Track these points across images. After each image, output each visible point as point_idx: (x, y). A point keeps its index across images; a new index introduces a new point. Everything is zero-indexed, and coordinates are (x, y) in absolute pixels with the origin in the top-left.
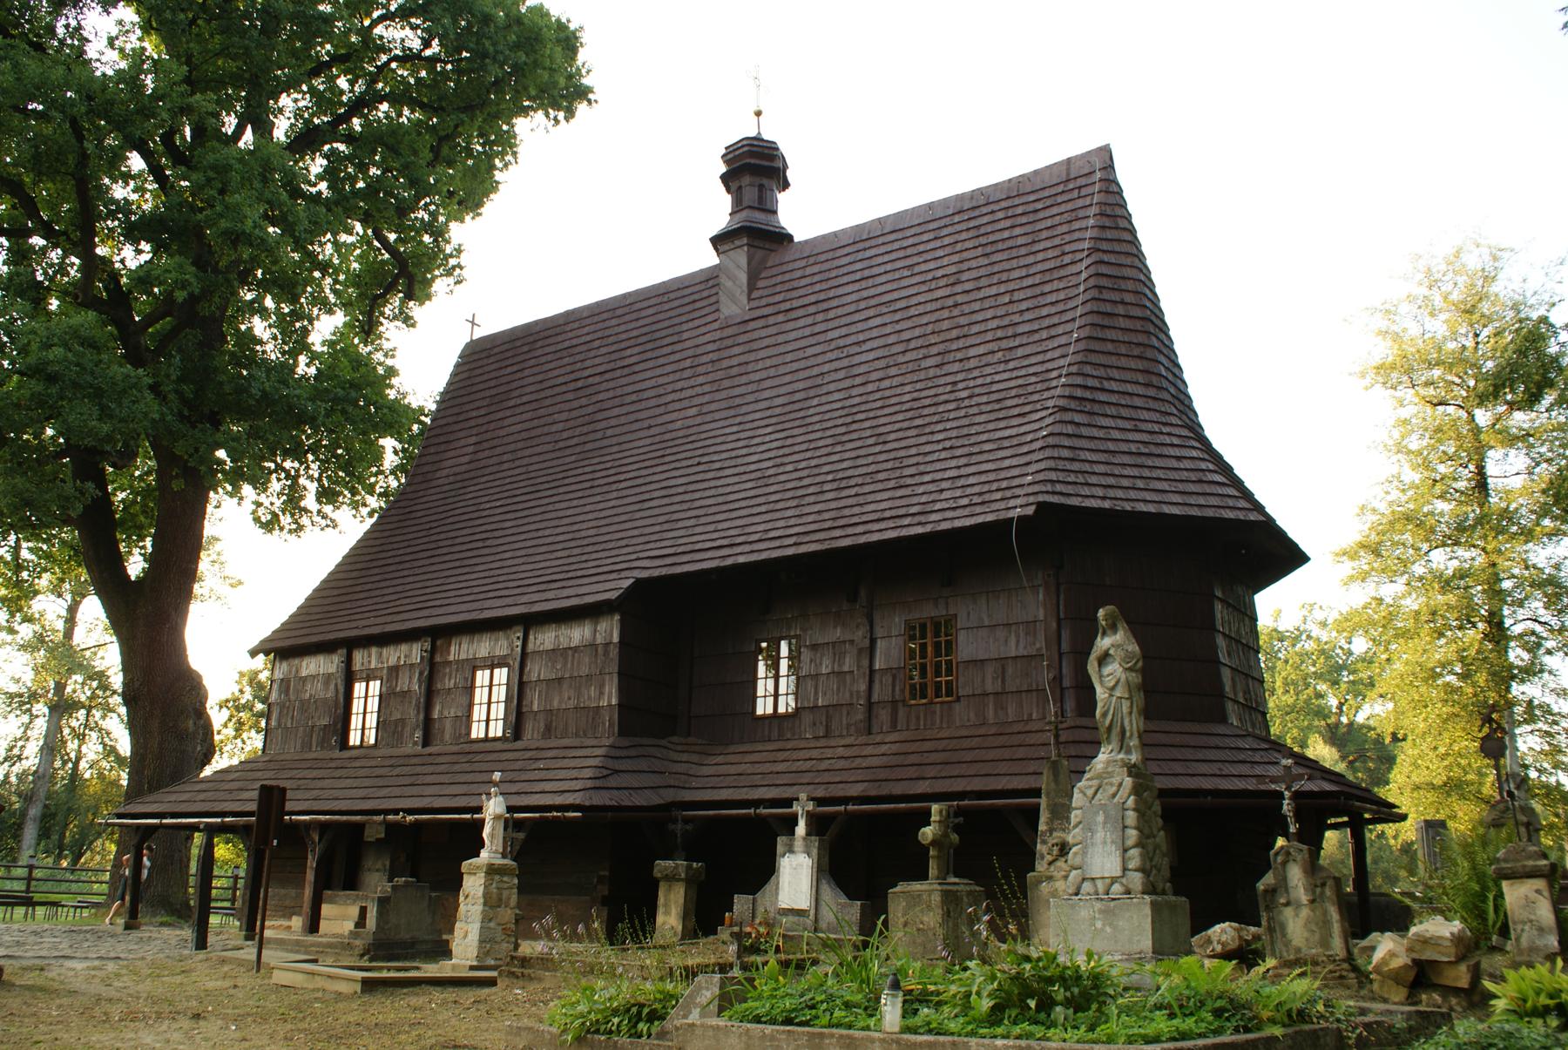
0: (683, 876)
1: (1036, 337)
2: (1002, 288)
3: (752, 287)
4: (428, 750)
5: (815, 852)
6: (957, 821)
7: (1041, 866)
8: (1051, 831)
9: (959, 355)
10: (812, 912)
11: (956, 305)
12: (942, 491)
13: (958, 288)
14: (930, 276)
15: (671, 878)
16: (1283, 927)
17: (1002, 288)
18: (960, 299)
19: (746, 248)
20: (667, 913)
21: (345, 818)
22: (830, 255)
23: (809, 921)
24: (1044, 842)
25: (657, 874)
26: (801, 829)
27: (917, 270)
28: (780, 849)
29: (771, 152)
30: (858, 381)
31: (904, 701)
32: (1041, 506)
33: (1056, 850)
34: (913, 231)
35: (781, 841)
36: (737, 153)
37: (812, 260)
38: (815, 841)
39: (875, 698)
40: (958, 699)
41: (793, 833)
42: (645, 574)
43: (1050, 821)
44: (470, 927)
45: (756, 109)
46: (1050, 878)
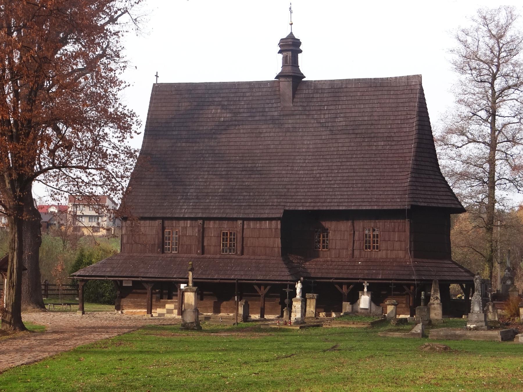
0: (316, 298)
3: (294, 97)
5: (370, 295)
7: (431, 301)
8: (434, 294)
11: (372, 124)
12: (380, 195)
16: (488, 316)
18: (374, 122)
19: (291, 82)
20: (310, 307)
23: (369, 311)
26: (365, 290)
28: (360, 294)
32: (412, 206)
33: (435, 299)
39: (355, 248)
40: (380, 251)
42: (287, 208)
43: (434, 292)
44: (297, 314)
45: (290, 23)
46: (434, 304)
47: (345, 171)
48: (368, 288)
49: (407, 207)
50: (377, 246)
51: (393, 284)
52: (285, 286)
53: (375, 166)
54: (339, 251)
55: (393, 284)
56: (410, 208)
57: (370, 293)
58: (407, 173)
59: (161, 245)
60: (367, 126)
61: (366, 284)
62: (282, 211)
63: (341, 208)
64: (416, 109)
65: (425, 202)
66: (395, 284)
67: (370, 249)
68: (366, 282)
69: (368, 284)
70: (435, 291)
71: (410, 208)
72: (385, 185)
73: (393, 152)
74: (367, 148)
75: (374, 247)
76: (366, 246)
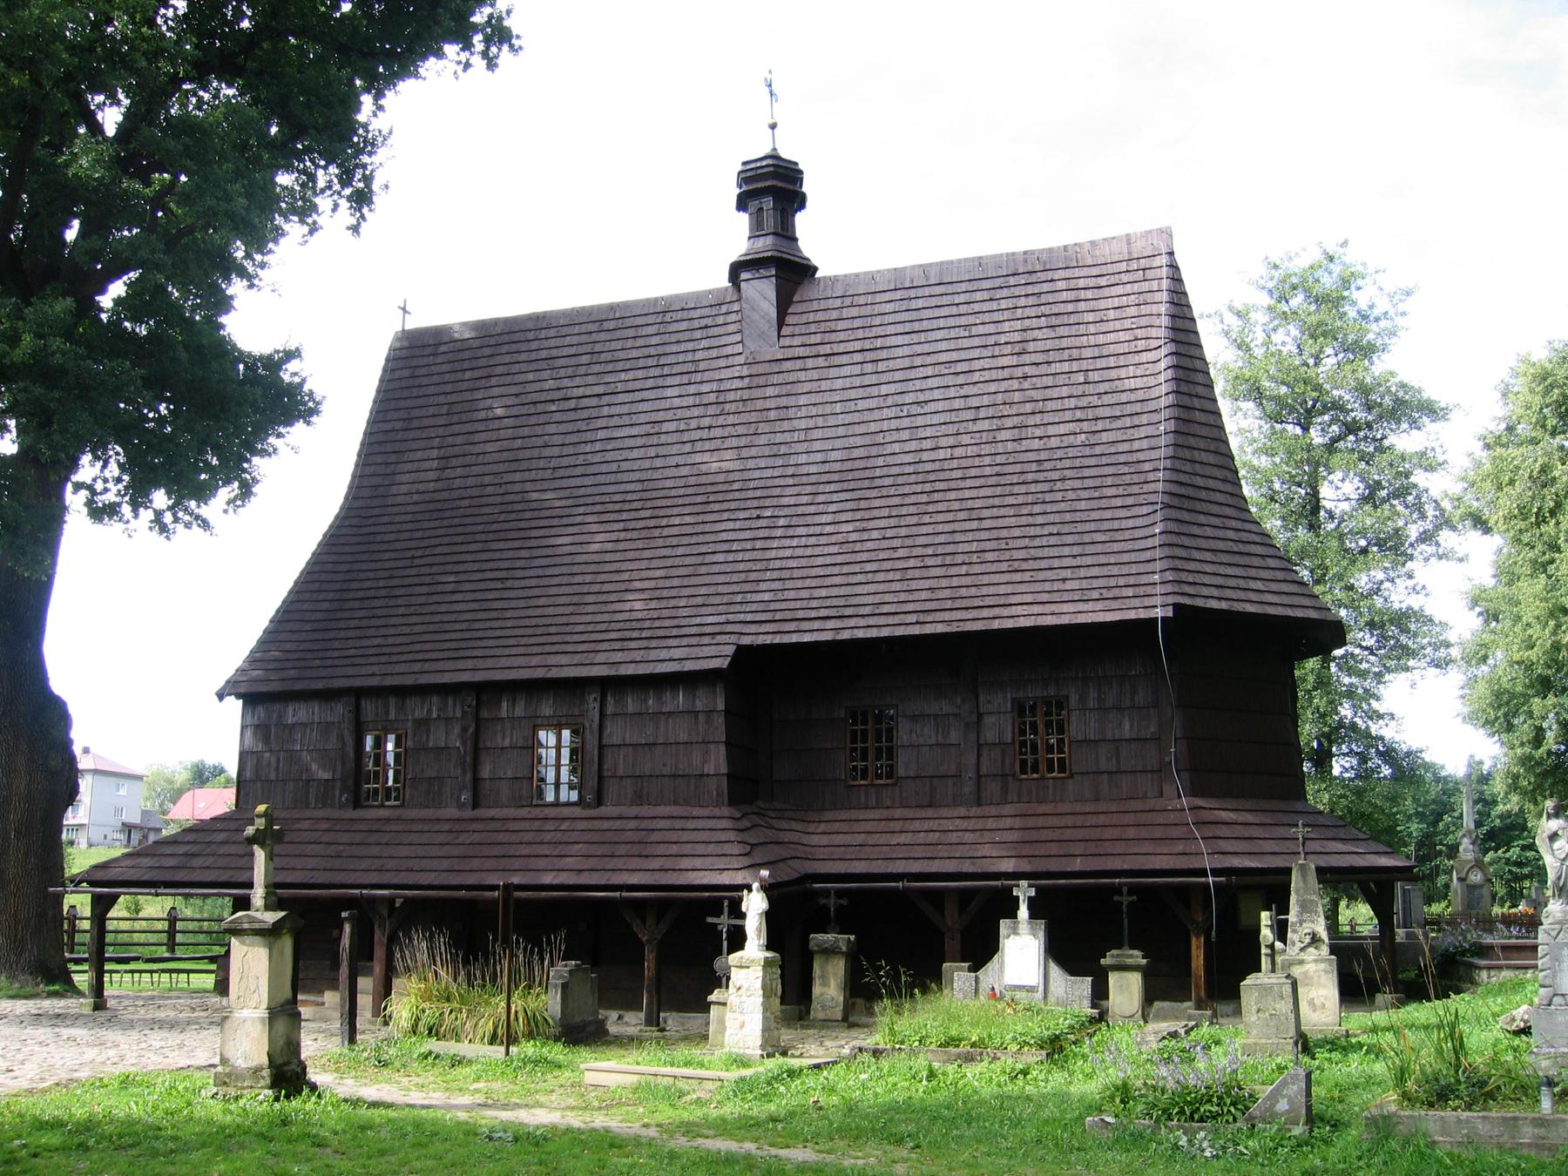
0: (844, 949)
1: (1119, 424)
2: (1075, 366)
3: (781, 323)
4: (479, 813)
5: (1041, 934)
6: (1130, 899)
9: (1038, 432)
10: (1041, 988)
11: (1026, 377)
12: (1064, 580)
13: (1027, 359)
14: (991, 340)
15: (829, 952)
17: (1075, 366)
18: (1029, 370)
19: (774, 279)
20: (825, 984)
21: (442, 893)
22: (870, 299)
24: (1295, 931)
25: (812, 946)
26: (1023, 912)
27: (974, 331)
28: (1003, 930)
29: (791, 174)
30: (927, 444)
31: (1014, 775)
33: (1307, 940)
34: (964, 287)
35: (1004, 925)
36: (760, 171)
37: (848, 301)
38: (1041, 924)
39: (984, 771)
40: (1071, 776)
41: (1015, 917)
42: (746, 641)
43: (1301, 913)
44: (747, 1018)
45: (772, 121)
46: (1301, 962)
47: (941, 517)
48: (1032, 903)
49: (1159, 613)
50: (1061, 761)
51: (1125, 889)
52: (715, 907)
53: (1039, 496)
54: (931, 783)
55: (1125, 889)
56: (1170, 614)
57: (1041, 924)
58: (1150, 509)
59: (350, 782)
60: (1010, 382)
61: (1024, 892)
62: (730, 650)
63: (928, 629)
64: (1165, 321)
65: (1220, 599)
66: (1133, 889)
67: (1035, 769)
68: (1023, 883)
69: (1032, 892)
70: (1305, 907)
71: (1170, 614)
72: (1076, 550)
73: (1098, 450)
74: (1010, 446)
75: (1050, 763)
76: (1023, 763)
